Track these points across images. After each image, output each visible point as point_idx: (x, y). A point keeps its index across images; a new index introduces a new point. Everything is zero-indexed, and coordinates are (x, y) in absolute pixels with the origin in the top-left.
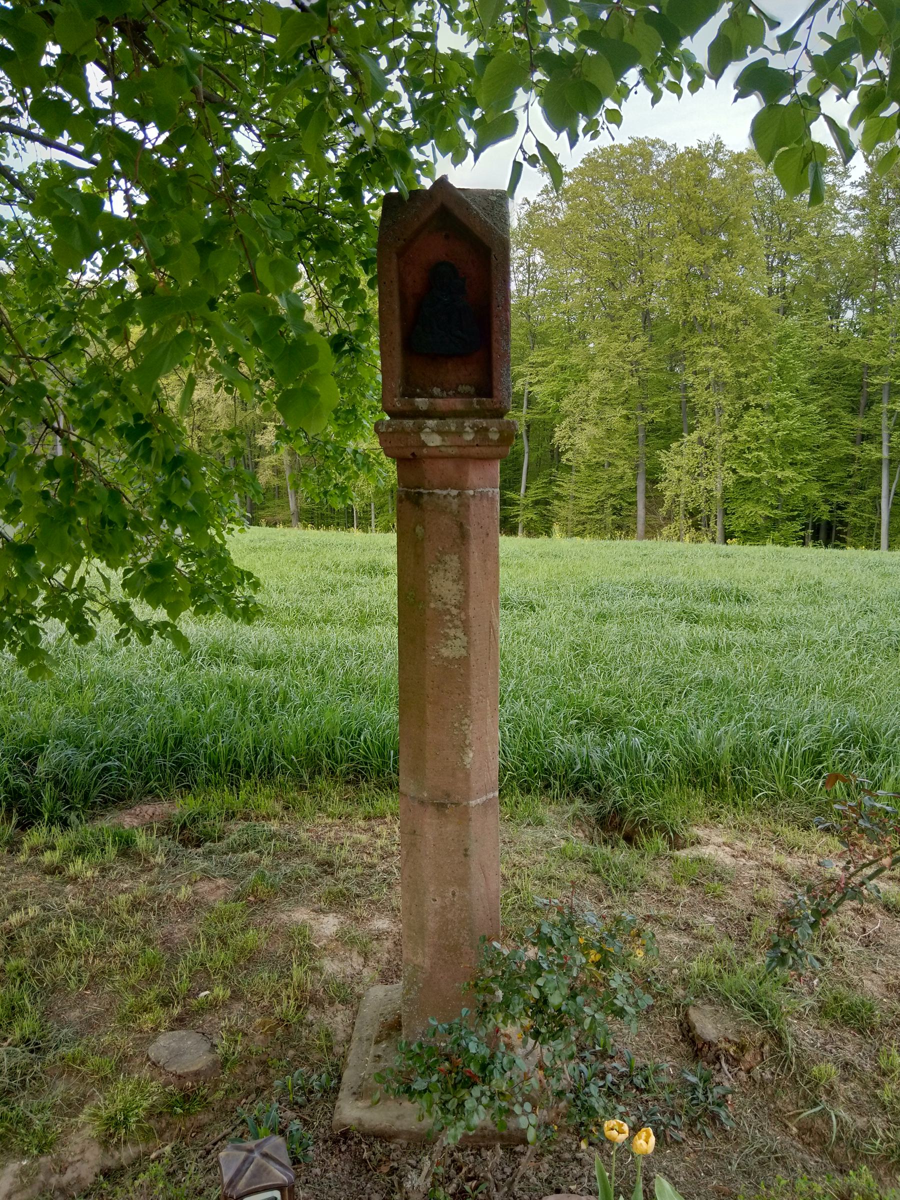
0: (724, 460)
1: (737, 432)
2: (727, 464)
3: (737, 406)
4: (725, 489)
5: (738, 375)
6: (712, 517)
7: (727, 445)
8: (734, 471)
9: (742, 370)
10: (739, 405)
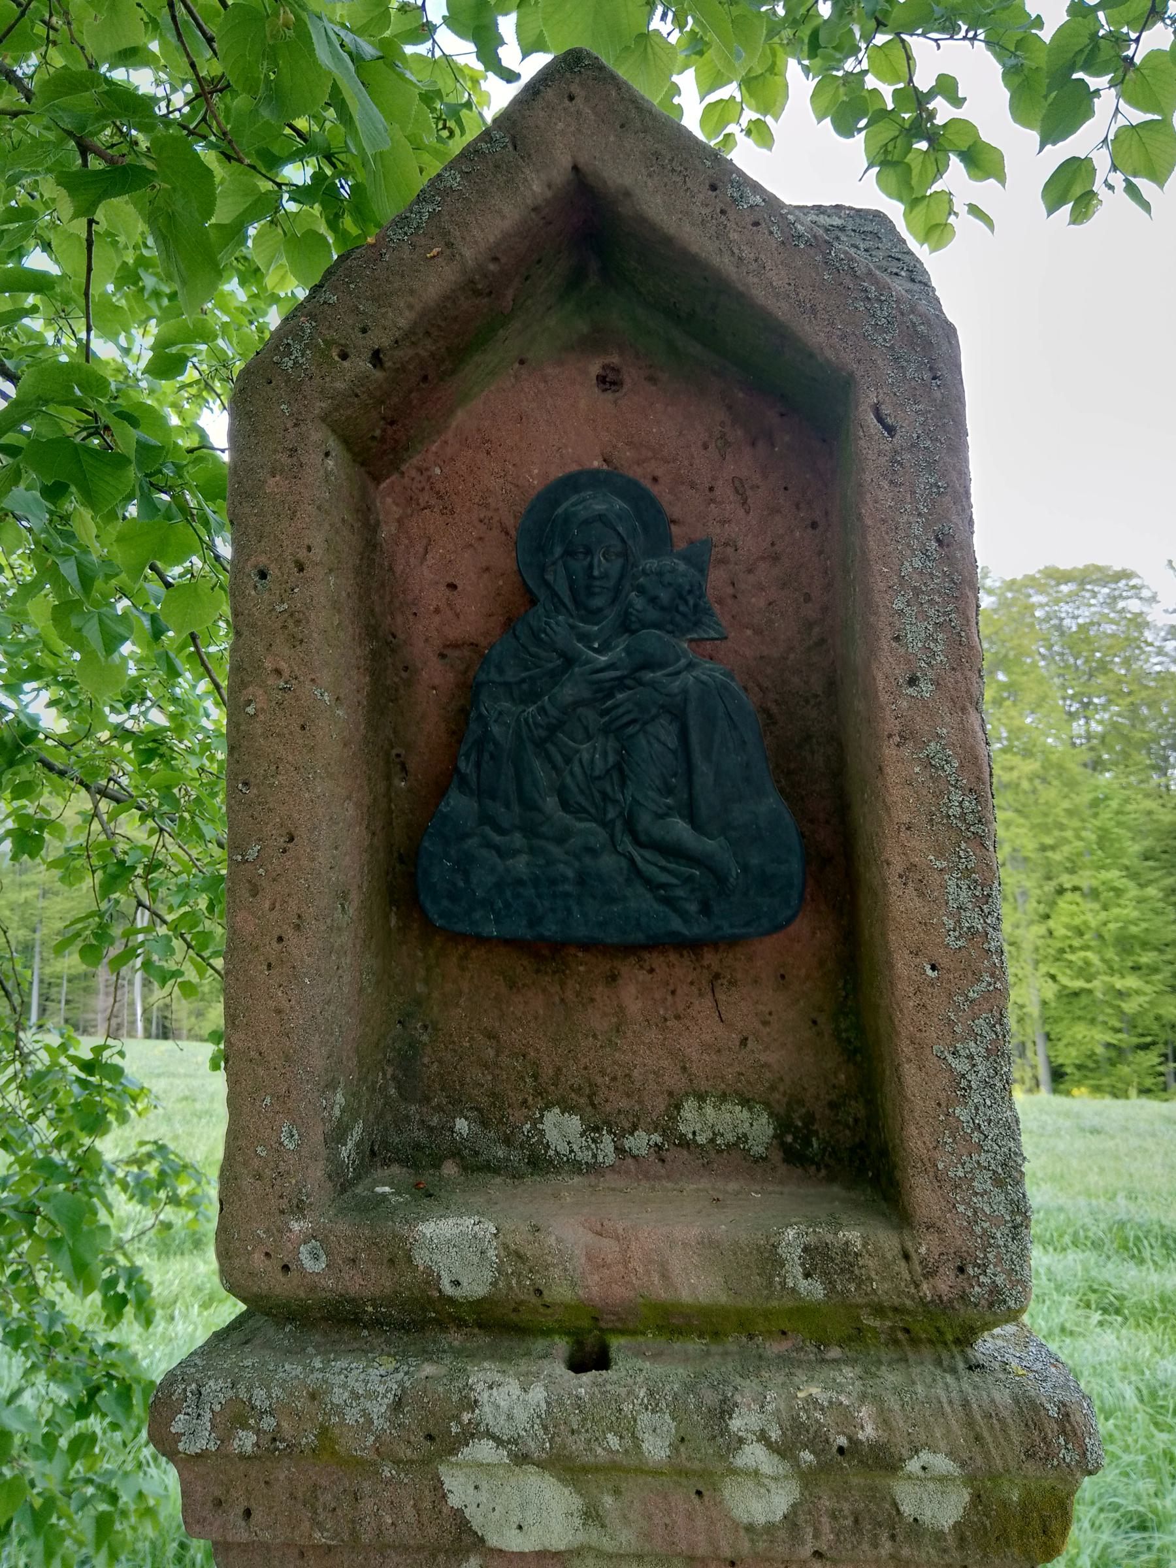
0: (1037, 963)
1: (1051, 923)
2: (1043, 969)
3: (1046, 889)
4: (1044, 1003)
5: (1043, 848)
6: (1029, 1045)
7: (1040, 942)
8: (1053, 978)
9: (1049, 841)
10: (1050, 887)
